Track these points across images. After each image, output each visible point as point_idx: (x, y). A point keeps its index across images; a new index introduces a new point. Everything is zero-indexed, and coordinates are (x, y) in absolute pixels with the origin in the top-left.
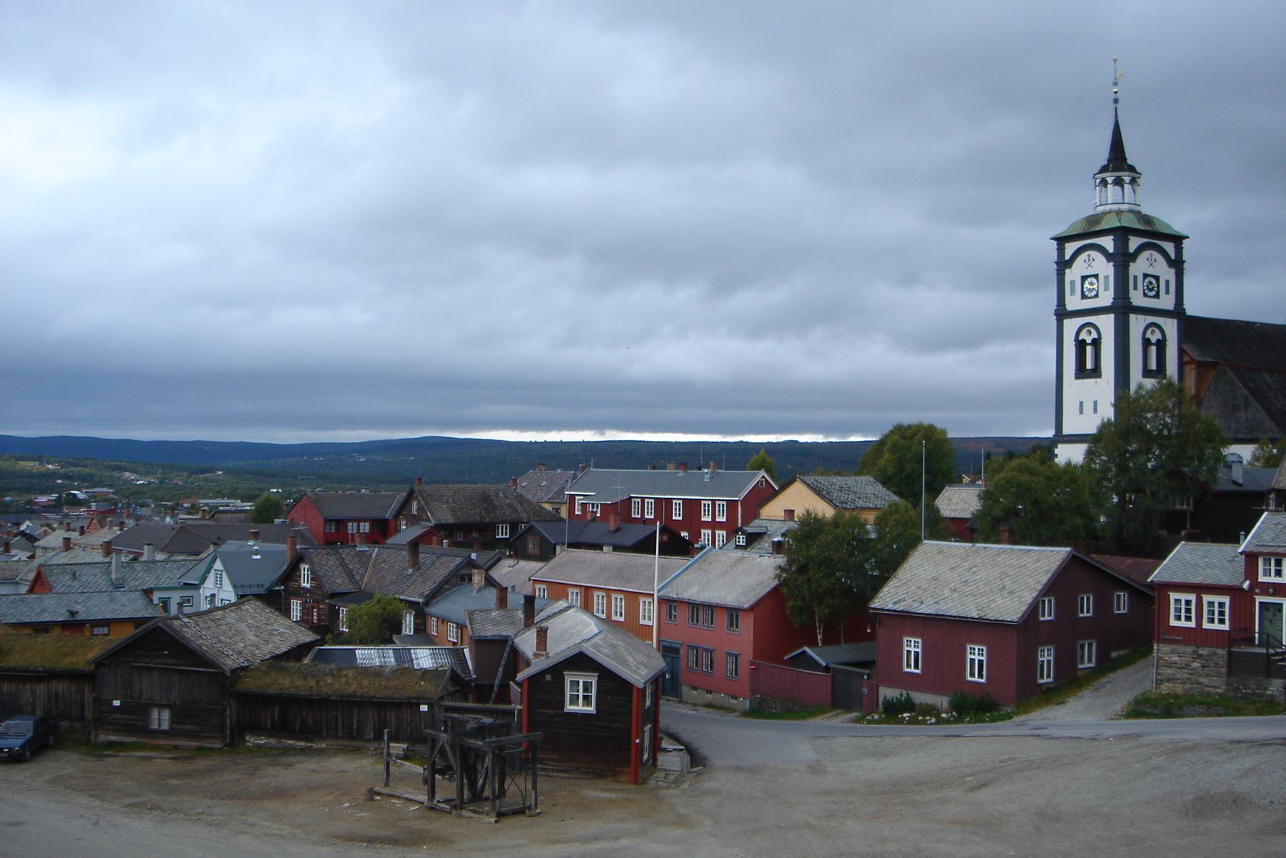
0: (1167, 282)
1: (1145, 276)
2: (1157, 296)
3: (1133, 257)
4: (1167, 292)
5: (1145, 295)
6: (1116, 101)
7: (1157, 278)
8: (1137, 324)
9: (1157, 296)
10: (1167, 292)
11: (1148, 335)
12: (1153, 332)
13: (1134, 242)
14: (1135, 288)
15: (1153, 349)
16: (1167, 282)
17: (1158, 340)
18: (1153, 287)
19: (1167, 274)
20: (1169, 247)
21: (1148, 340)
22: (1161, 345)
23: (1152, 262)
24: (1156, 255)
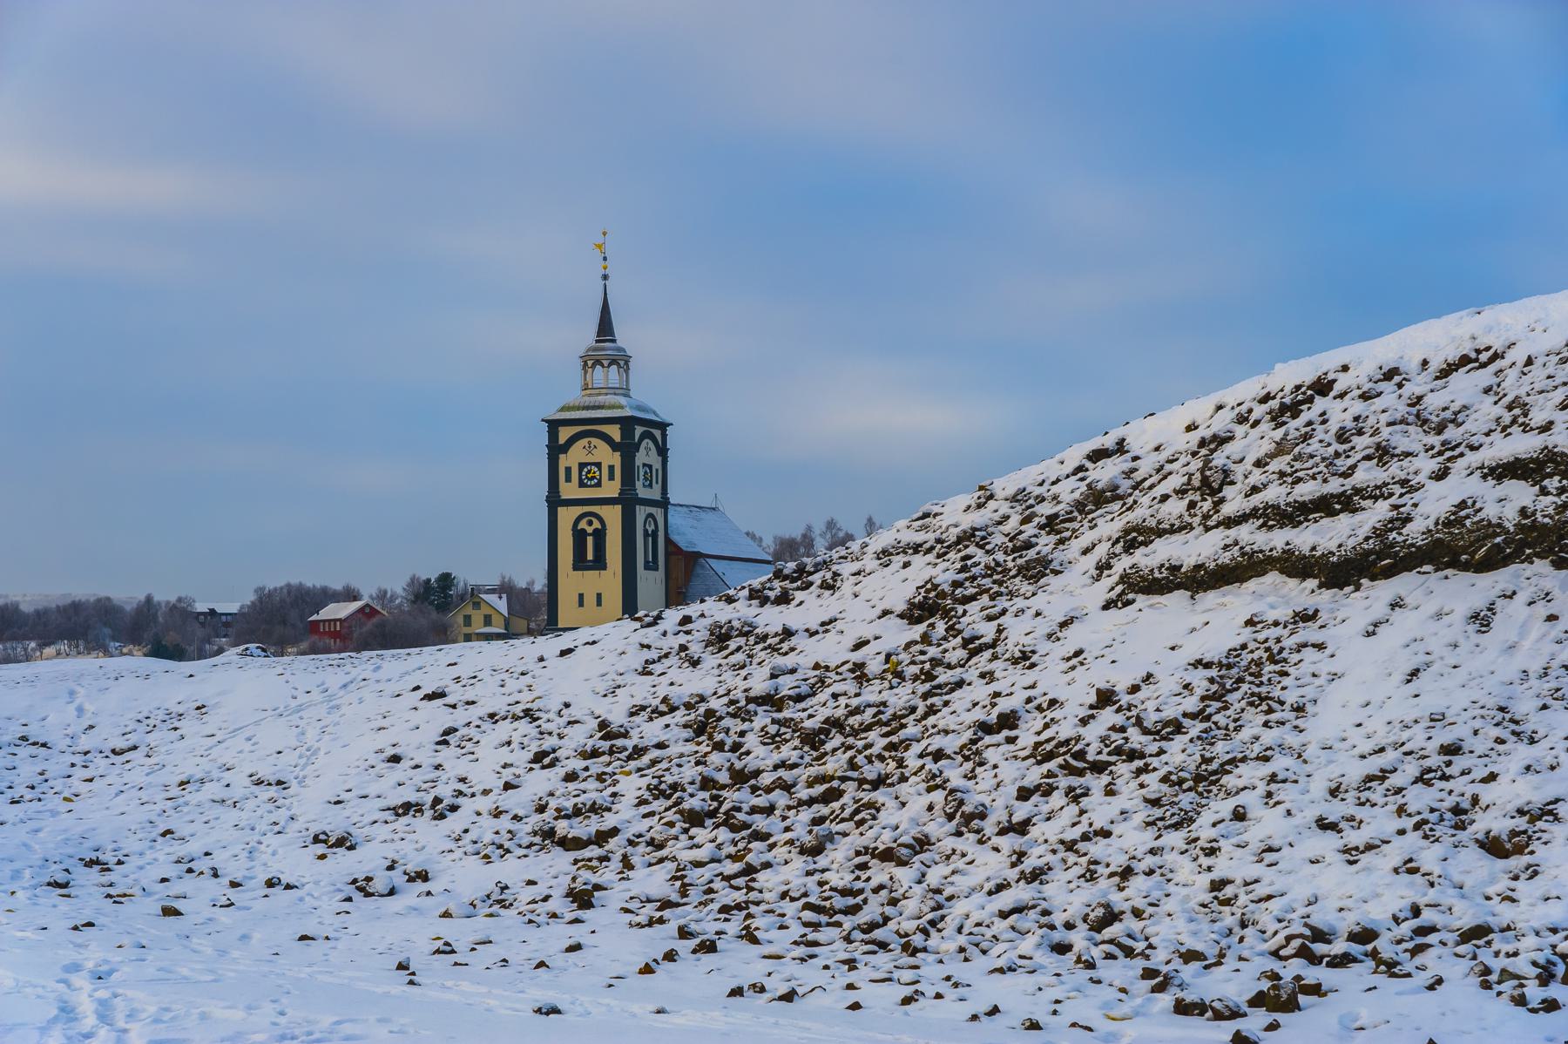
0: (611, 468)
1: (582, 466)
2: (599, 485)
3: (565, 448)
4: (611, 478)
5: (582, 485)
6: (605, 277)
7: (598, 465)
8: (566, 516)
9: (599, 485)
10: (611, 478)
11: (583, 525)
12: (590, 523)
13: (564, 434)
14: (568, 479)
15: (590, 540)
16: (611, 468)
17: (596, 530)
18: (588, 474)
19: (609, 457)
20: (615, 432)
21: (583, 530)
22: (600, 535)
23: (590, 449)
24: (595, 441)
